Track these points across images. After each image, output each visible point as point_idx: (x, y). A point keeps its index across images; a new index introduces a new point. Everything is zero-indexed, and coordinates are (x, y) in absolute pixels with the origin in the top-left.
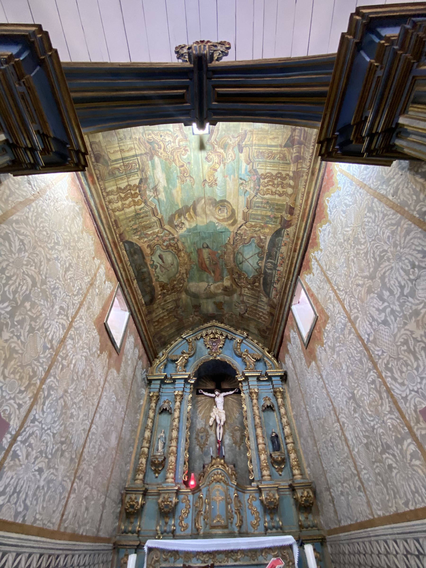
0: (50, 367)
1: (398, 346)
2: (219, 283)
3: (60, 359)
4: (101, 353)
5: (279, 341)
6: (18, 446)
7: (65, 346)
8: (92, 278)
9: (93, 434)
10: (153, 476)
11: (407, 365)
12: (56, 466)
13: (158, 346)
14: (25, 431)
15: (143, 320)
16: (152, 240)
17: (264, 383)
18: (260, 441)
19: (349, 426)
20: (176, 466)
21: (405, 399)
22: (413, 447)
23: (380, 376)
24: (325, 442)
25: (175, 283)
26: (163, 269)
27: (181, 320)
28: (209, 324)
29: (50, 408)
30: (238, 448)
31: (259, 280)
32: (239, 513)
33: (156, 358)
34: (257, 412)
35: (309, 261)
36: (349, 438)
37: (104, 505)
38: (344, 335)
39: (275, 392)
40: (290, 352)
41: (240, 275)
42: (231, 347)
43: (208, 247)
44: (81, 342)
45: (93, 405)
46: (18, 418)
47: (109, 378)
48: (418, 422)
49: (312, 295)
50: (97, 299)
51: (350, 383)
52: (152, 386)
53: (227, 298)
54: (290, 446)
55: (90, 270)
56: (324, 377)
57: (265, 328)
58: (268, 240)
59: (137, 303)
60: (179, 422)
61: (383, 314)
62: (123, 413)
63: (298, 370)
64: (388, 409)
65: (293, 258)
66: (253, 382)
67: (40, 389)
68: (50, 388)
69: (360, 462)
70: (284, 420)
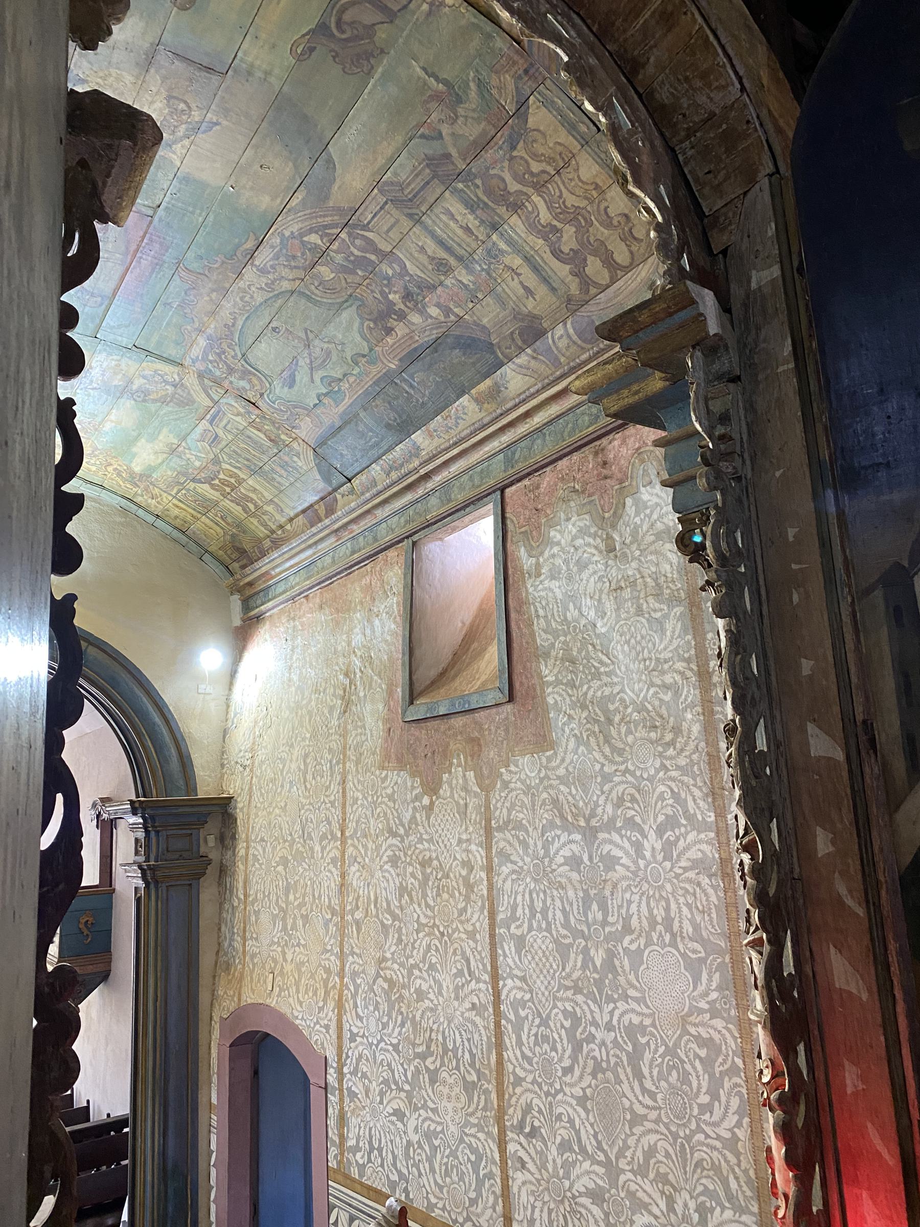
9: (518, 1004)
12: (430, 1104)
14: (347, 1057)
44: (370, 845)
45: (472, 935)
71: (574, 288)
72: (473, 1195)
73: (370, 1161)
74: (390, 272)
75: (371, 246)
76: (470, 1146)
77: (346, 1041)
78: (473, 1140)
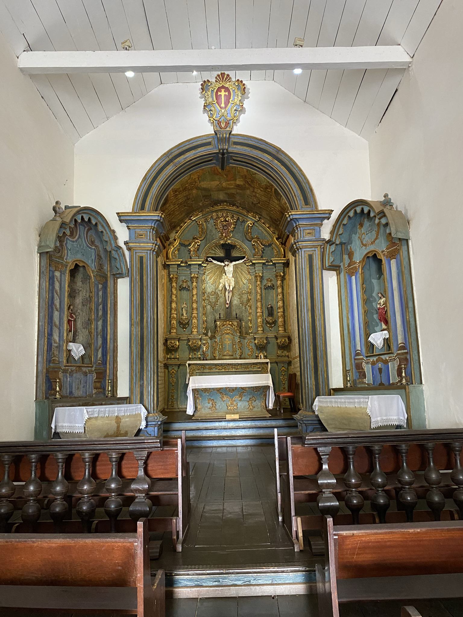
10: (182, 330)
17: (269, 267)
18: (259, 310)
28: (220, 207)
30: (244, 308)
34: (259, 291)
41: (252, 181)
52: (170, 269)
54: (279, 314)
60: (197, 298)
70: (280, 297)
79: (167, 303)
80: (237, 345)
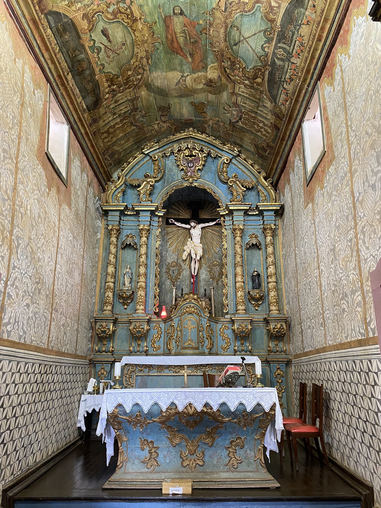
0: (13, 218)
1: (375, 214)
2: (199, 73)
3: (17, 208)
4: (50, 190)
5: (280, 166)
6: (10, 288)
7: (18, 192)
8: (21, 95)
9: (59, 273)
10: (122, 308)
11: (375, 233)
13: (110, 165)
15: (86, 133)
16: (88, 6)
18: (239, 279)
19: (325, 274)
20: (146, 299)
21: (366, 260)
22: (360, 298)
23: (356, 237)
24: (305, 285)
25: (130, 73)
26: (110, 53)
27: (141, 128)
28: (183, 135)
29: (22, 255)
30: (215, 284)
31: (263, 75)
32: (211, 338)
33: (109, 181)
34: (239, 250)
35: (333, 65)
36: (323, 284)
37: (77, 330)
38: (342, 184)
39: (265, 229)
40: (291, 184)
41: (233, 64)
42: (213, 168)
43: (182, 13)
44: (30, 184)
45: (54, 246)
46: (5, 268)
47: (62, 217)
48: (367, 281)
49: (327, 119)
50: (32, 124)
51: (335, 236)
52: (109, 218)
53: (211, 97)
54: (270, 285)
55: (16, 84)
56: (316, 223)
57: (265, 145)
58: (283, 11)
59: (76, 111)
61: (375, 177)
62: (81, 249)
63: (295, 208)
64: (354, 265)
65: (316, 50)
66: (239, 217)
67: (11, 241)
68: (18, 238)
69: (326, 304)
70: (270, 260)
71: (103, 131)
72: (42, 333)
73: (13, 328)
74: (121, 89)
75: (129, 88)
76: (45, 316)
77: (11, 269)
78: (46, 314)
79: (102, 268)
80: (205, 332)
